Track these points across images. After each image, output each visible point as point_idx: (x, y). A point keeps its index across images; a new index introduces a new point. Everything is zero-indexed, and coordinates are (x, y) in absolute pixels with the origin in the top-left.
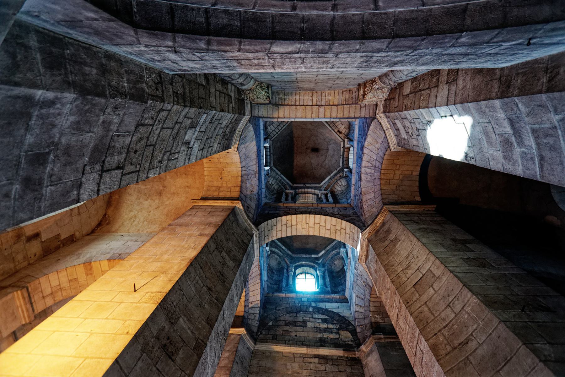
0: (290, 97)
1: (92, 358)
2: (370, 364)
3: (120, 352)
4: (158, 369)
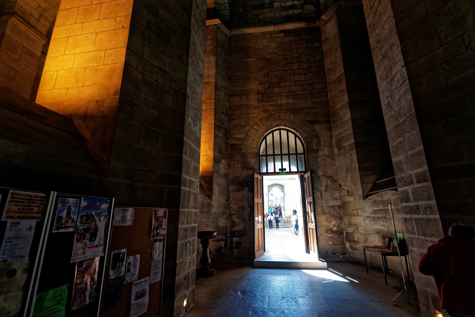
1: (110, 49)
3: (127, 42)
4: (162, 51)
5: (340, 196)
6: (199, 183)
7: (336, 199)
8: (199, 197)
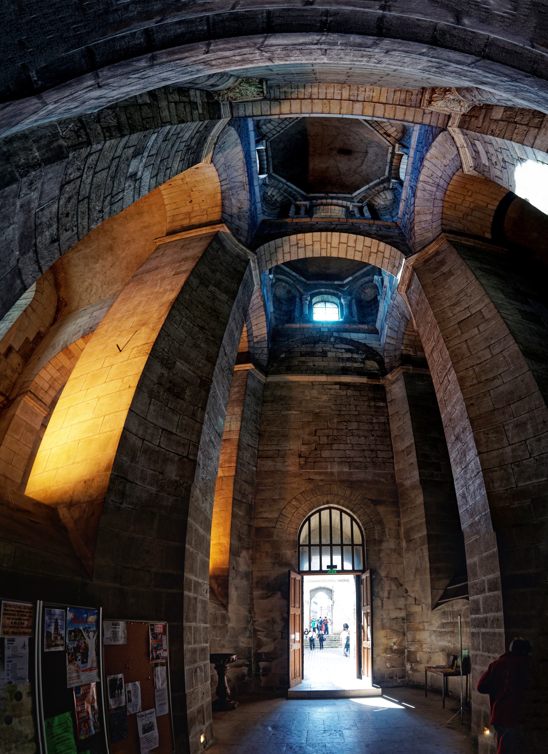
2: (393, 391)
5: (405, 605)
6: (208, 586)
7: (400, 609)
8: (209, 606)
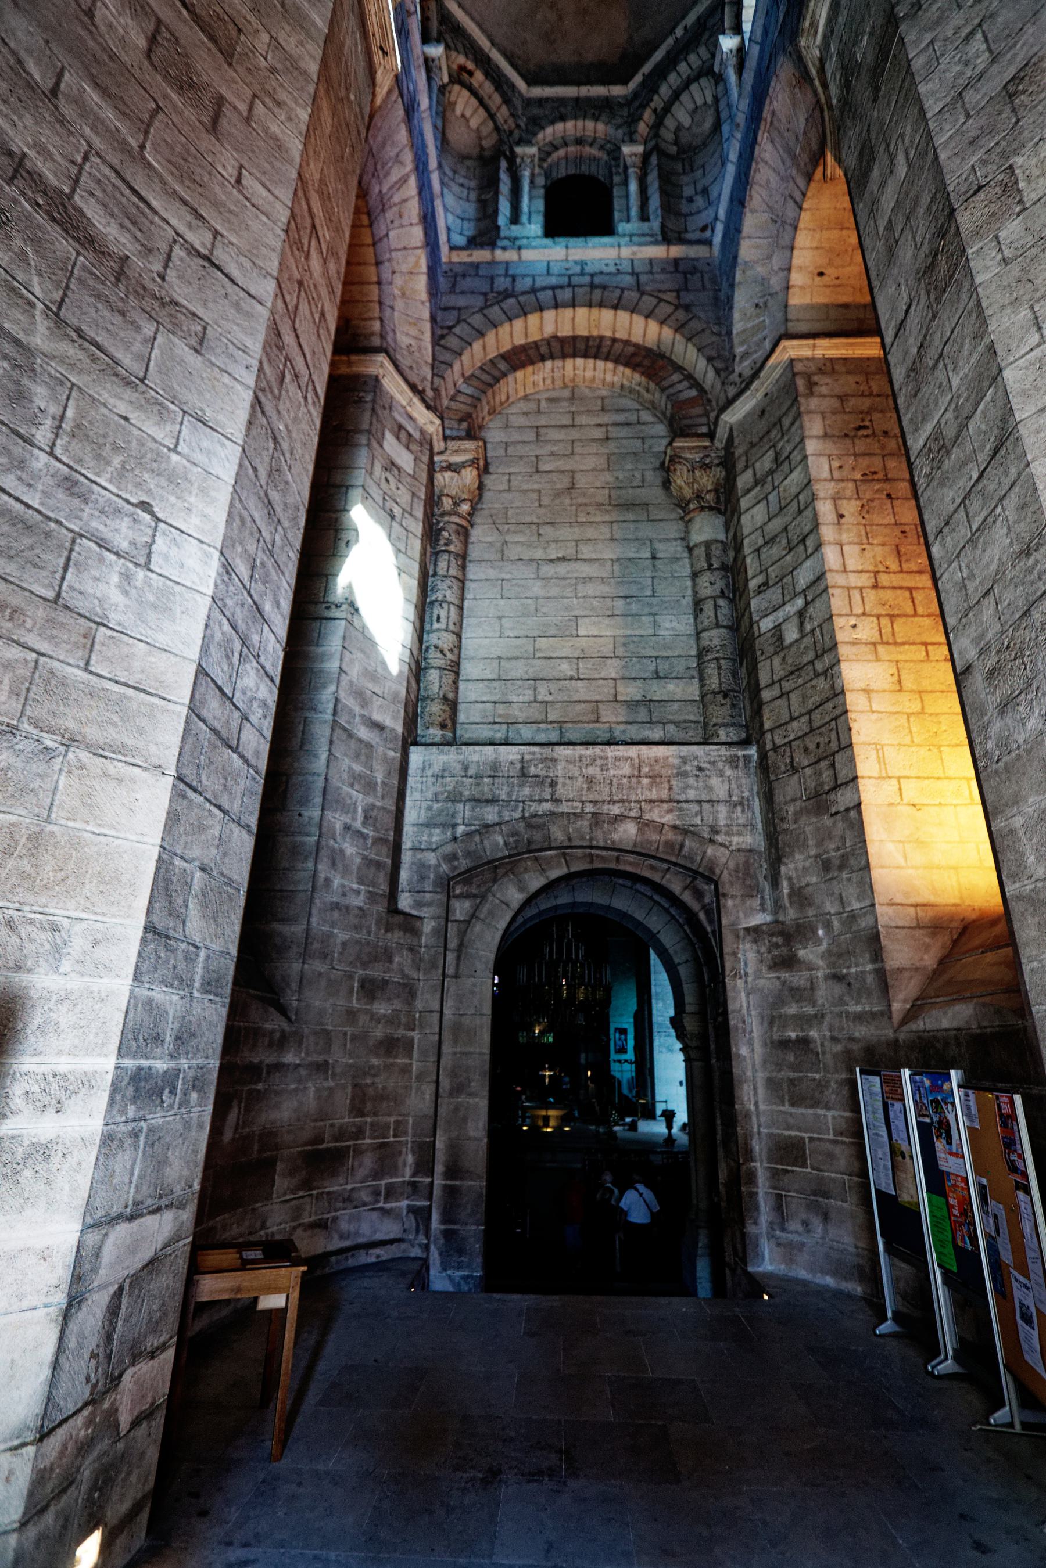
0: (625, 382)
